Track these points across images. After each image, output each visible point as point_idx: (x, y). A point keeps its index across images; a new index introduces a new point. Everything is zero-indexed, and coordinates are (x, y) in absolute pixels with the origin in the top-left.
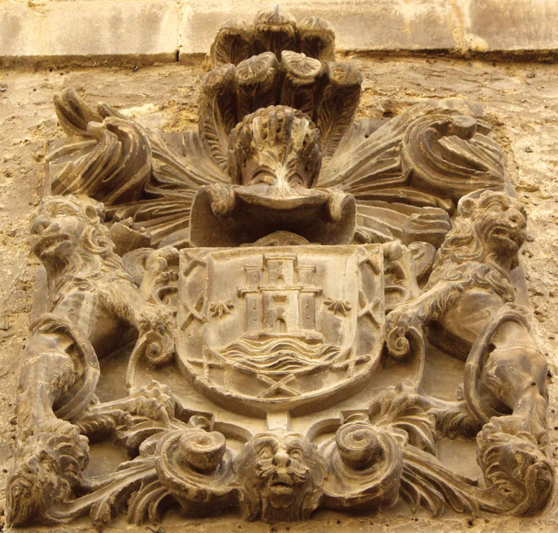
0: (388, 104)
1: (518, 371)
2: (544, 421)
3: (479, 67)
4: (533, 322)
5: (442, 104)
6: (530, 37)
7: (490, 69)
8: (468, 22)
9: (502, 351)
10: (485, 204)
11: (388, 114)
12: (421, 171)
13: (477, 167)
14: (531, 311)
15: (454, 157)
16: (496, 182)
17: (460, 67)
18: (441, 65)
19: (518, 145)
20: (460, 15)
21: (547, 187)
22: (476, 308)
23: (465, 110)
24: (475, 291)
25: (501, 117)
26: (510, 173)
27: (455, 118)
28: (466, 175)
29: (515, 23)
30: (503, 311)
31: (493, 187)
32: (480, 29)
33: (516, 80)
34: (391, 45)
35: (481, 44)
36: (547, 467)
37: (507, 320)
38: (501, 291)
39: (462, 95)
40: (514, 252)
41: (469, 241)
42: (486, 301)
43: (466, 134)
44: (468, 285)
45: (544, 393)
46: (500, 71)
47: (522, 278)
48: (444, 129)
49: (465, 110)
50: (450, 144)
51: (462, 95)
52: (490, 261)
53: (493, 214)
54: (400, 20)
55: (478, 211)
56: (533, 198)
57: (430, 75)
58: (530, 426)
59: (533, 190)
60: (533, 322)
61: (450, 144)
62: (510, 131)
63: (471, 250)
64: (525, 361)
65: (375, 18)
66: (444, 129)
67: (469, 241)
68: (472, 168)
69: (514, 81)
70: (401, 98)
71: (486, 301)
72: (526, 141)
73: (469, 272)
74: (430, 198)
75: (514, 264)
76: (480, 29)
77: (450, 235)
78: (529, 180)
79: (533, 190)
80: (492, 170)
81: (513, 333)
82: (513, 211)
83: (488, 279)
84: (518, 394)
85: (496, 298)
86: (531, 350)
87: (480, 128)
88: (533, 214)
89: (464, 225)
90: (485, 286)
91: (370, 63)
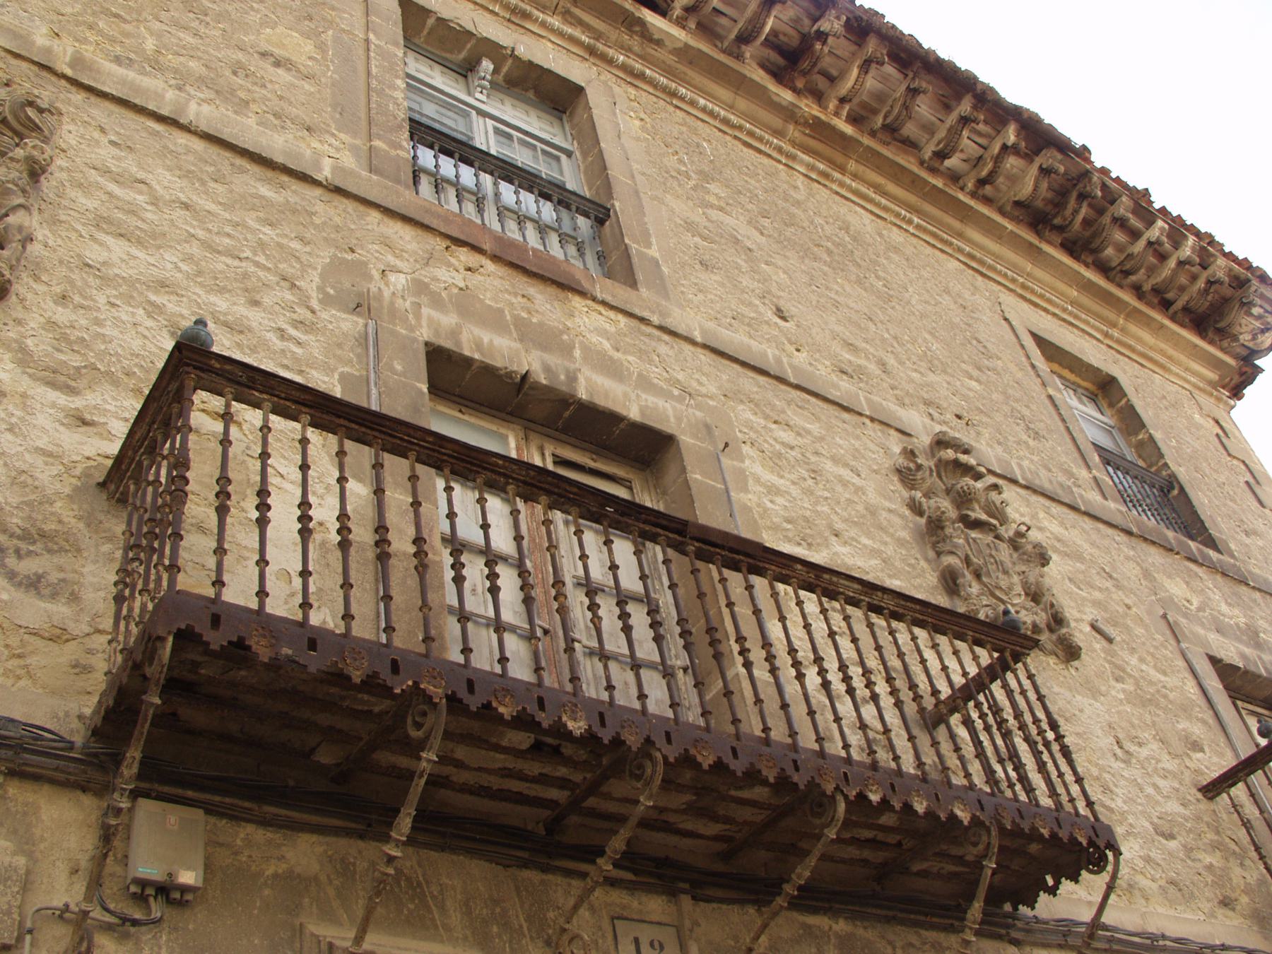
0: (9, 80)
1: (15, 232)
2: (18, 260)
3: (63, 82)
4: (35, 213)
5: (36, 92)
6: (95, 80)
7: (68, 86)
8: (68, 59)
9: (11, 219)
10: (34, 147)
11: (7, 85)
12: (10, 118)
13: (39, 128)
14: (36, 206)
15: (29, 119)
16: (46, 140)
17: (54, 79)
18: (45, 74)
19: (65, 127)
20: (65, 54)
21: (71, 153)
22: (8, 194)
23: (46, 100)
24: (10, 186)
25: (64, 110)
26: (56, 138)
27: (39, 101)
28: (33, 130)
29: (91, 70)
30: (21, 201)
31: (43, 142)
32: (72, 65)
33: (79, 97)
34: (23, 53)
35: (69, 72)
36: (9, 281)
37: (21, 206)
38: (24, 191)
39: (47, 92)
40: (39, 175)
41: (18, 161)
42: (14, 192)
43: (41, 111)
44: (8, 182)
45: (24, 247)
46: (74, 89)
47: (38, 190)
48: (31, 104)
49: (46, 100)
50: (30, 112)
51: (47, 92)
52: (25, 175)
53: (35, 153)
54: (33, 43)
55: (29, 149)
56: (62, 155)
57: (37, 76)
58: (9, 259)
59: (64, 151)
60: (35, 213)
61: (30, 112)
62: (65, 119)
63: (18, 166)
64: (20, 229)
65: (21, 37)
66: (31, 104)
67: (18, 161)
68: (37, 128)
69: (78, 97)
70: (17, 80)
71: (14, 192)
72: (71, 127)
73: (12, 176)
74: (10, 134)
75: (37, 181)
76: (72, 65)
77: (10, 155)
78: (64, 146)
79: (64, 151)
80: (46, 132)
81: (22, 212)
82: (46, 156)
83: (20, 183)
84: (11, 242)
85: (19, 193)
86: (26, 224)
87: (49, 111)
88: (59, 162)
89: (19, 153)
90: (17, 185)
91: (9, 56)
